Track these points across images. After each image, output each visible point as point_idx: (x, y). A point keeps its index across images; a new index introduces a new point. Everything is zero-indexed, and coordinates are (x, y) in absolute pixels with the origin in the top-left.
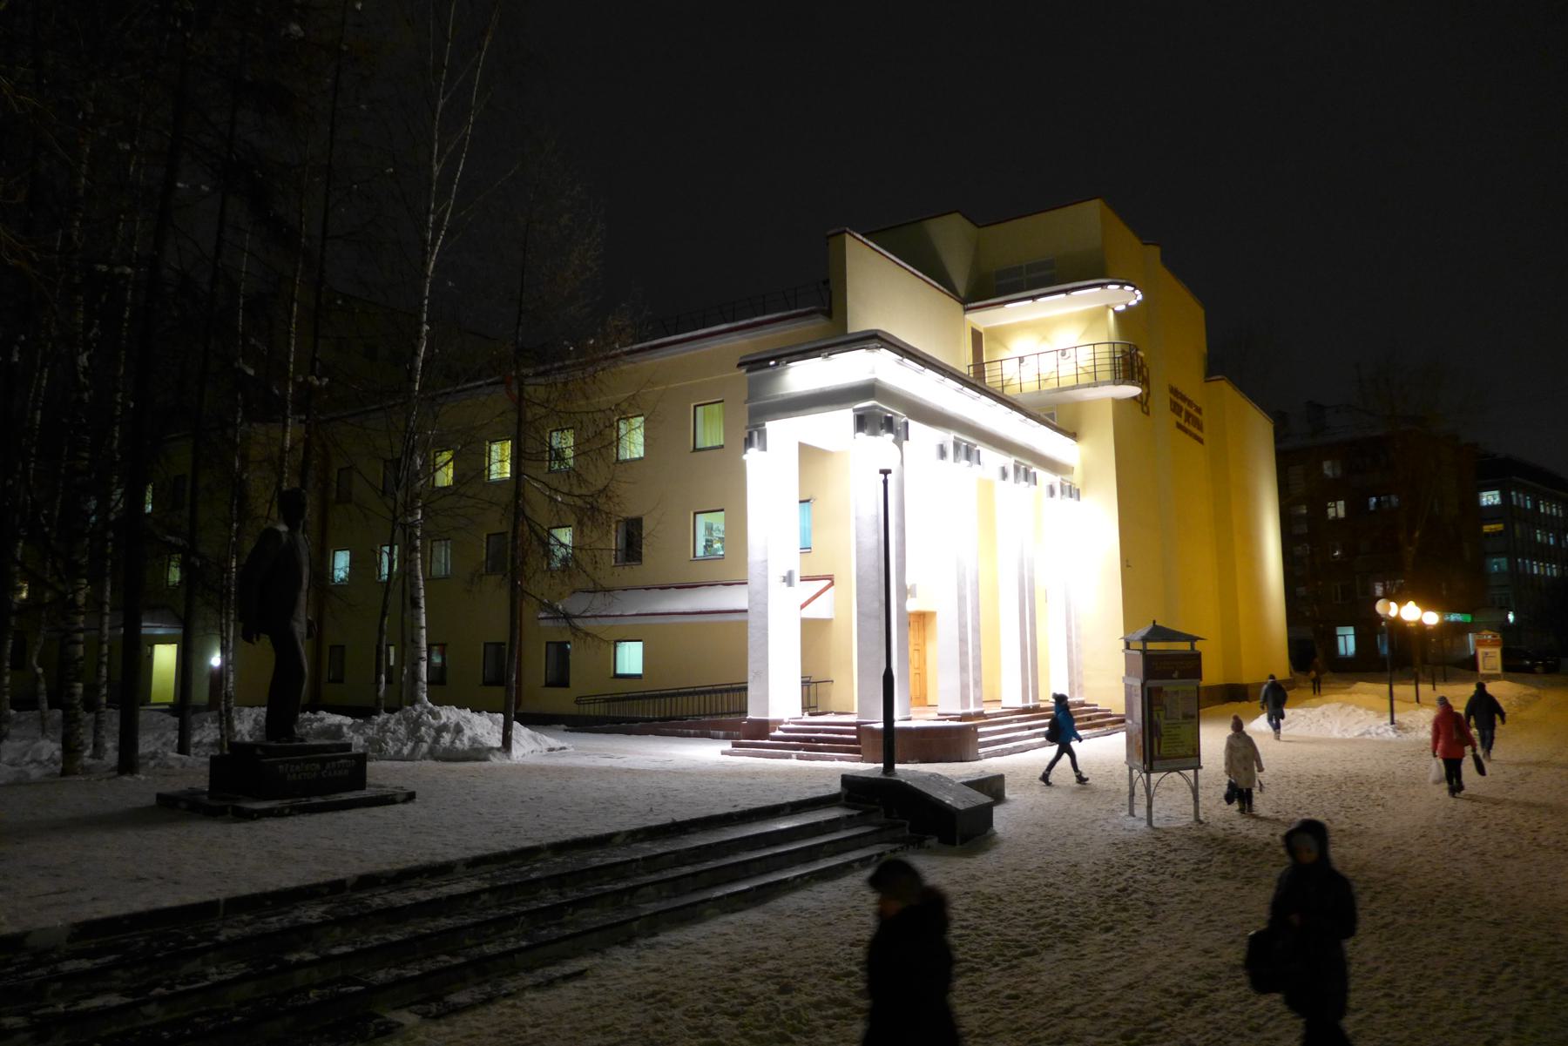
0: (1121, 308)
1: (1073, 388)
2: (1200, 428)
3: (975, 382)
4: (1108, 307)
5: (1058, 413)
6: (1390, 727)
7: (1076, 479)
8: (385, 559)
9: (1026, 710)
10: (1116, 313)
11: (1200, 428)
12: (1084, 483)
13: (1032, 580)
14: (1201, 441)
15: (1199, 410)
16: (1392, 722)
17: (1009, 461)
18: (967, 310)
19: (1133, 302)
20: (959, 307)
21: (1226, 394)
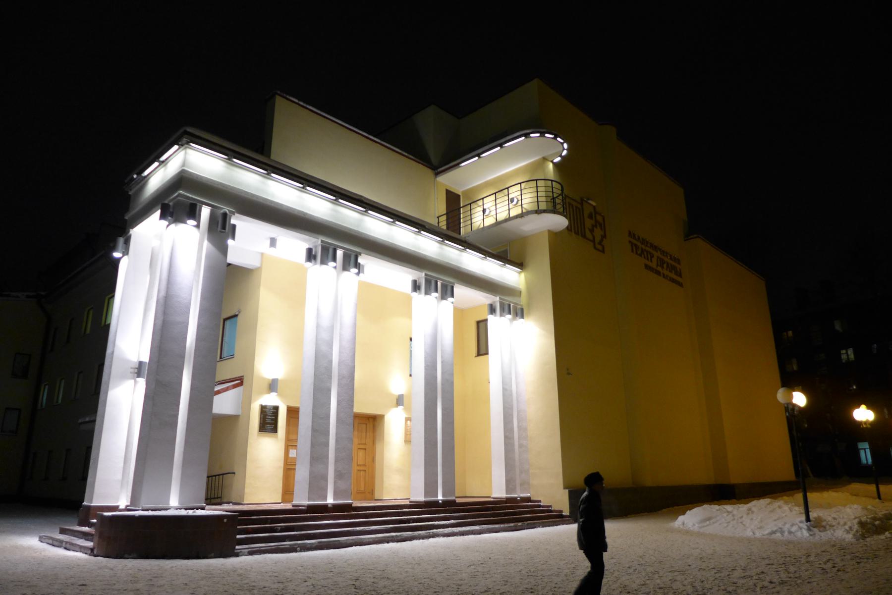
0: (558, 159)
1: (506, 220)
2: (680, 276)
3: (451, 230)
4: (545, 159)
5: (503, 246)
6: (804, 525)
7: (523, 301)
8: (58, 384)
9: (427, 504)
10: (554, 164)
11: (680, 276)
12: (529, 305)
13: (449, 385)
14: (680, 285)
15: (678, 261)
16: (808, 519)
17: (420, 275)
18: (437, 174)
19: (565, 153)
20: (429, 172)
21: (701, 246)
